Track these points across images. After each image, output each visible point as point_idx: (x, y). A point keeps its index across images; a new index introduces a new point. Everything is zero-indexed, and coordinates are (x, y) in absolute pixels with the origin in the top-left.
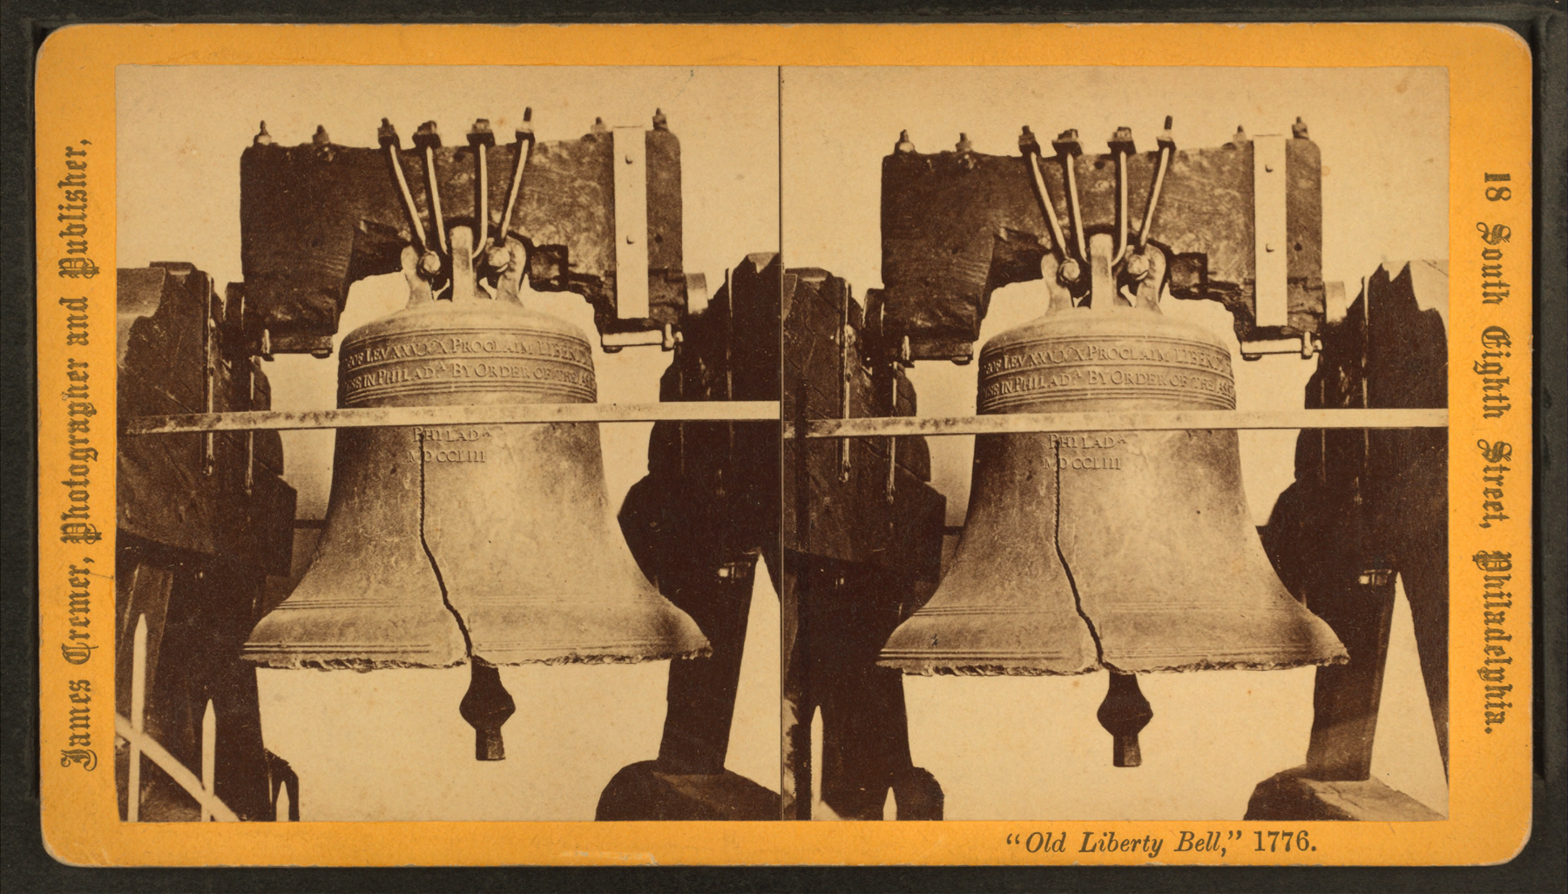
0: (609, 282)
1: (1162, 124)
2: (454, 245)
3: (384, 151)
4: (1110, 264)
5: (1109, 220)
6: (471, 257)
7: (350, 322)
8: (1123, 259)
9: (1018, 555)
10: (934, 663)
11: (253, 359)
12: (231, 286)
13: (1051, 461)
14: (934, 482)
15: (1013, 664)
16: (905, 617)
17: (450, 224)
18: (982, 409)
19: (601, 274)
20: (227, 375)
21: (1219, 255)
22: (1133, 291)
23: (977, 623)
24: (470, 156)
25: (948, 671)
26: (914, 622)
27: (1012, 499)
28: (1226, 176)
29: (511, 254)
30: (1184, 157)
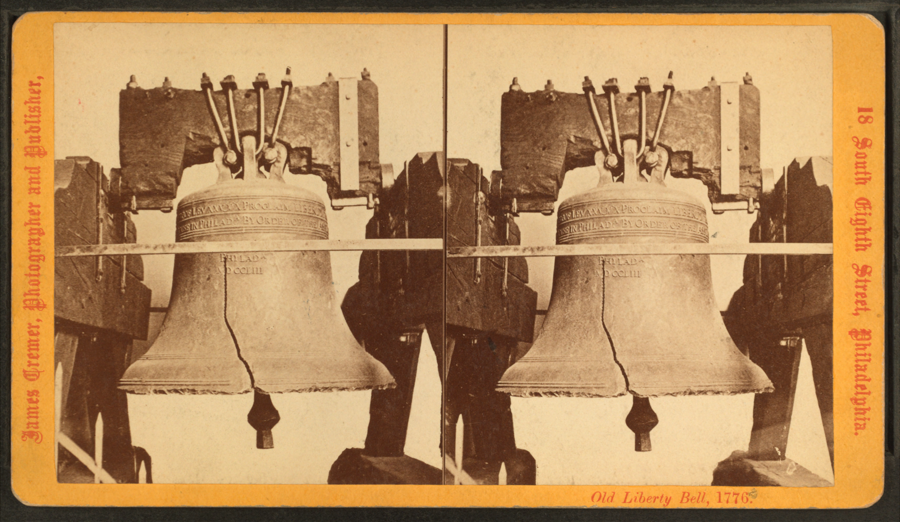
0: (336, 169)
1: (667, 75)
2: (245, 147)
3: (204, 92)
4: (636, 157)
5: (635, 131)
6: (255, 154)
7: (183, 192)
8: (643, 154)
9: (580, 327)
10: (529, 390)
11: (126, 213)
12: (113, 170)
13: (600, 272)
14: (530, 284)
15: (576, 391)
16: (513, 362)
17: (242, 135)
18: (558, 242)
19: (331, 164)
20: (111, 222)
21: (699, 152)
22: (649, 173)
23: (554, 366)
24: (254, 95)
25: (537, 394)
26: (518, 366)
27: (576, 294)
28: (704, 106)
29: (278, 152)
30: (680, 95)
